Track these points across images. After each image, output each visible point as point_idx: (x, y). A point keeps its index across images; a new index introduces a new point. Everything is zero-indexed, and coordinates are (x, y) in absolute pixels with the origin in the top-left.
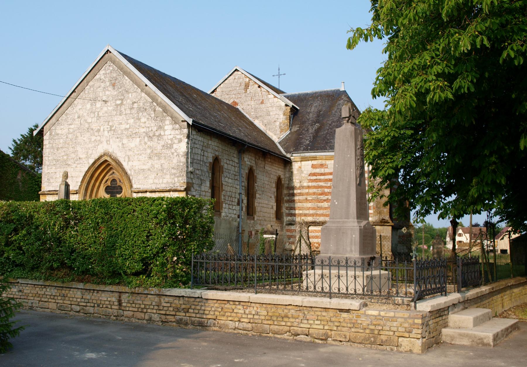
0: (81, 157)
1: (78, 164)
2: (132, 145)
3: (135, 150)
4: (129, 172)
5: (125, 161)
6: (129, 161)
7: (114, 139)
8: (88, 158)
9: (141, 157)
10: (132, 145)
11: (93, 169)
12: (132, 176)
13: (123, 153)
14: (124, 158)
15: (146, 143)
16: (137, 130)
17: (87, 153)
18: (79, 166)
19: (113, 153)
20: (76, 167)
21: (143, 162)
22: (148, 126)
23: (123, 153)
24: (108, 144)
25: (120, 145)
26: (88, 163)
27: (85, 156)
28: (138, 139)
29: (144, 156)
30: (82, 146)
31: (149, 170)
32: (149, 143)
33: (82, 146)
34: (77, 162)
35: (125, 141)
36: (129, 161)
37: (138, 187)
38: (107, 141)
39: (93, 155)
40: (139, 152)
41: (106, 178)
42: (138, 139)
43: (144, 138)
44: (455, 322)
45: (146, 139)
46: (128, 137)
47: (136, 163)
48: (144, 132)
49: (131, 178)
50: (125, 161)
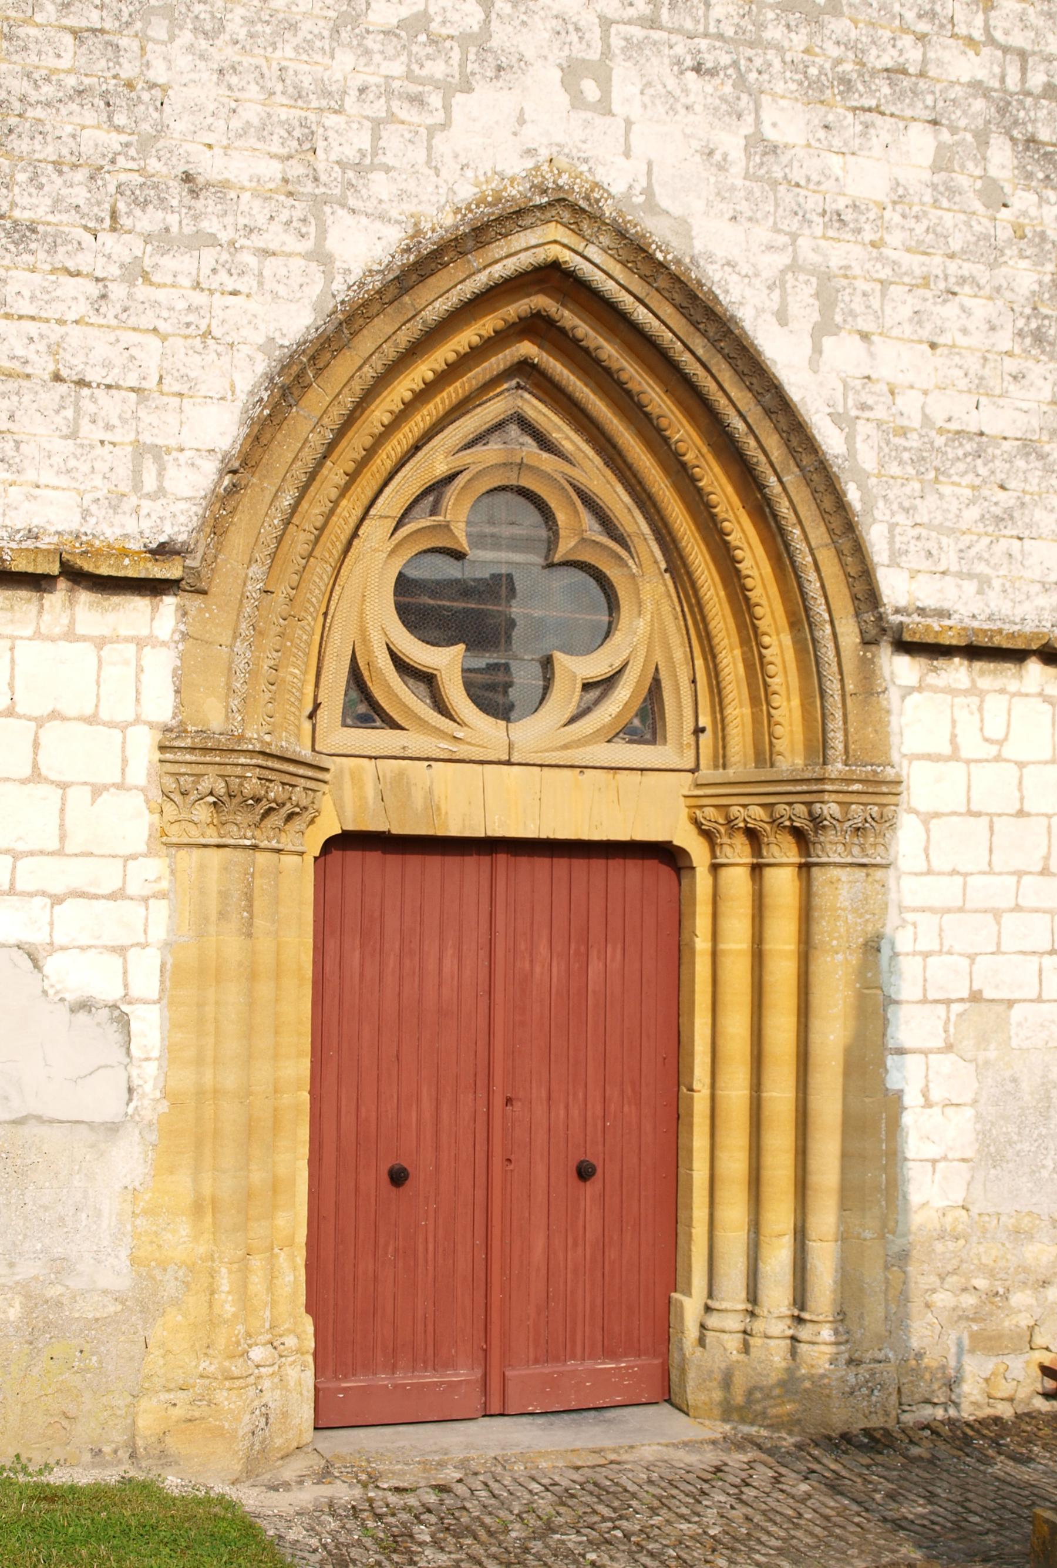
0: (210, 166)
1: (162, 240)
2: (865, 178)
3: (895, 239)
4: (831, 440)
5: (782, 318)
6: (825, 328)
7: (659, 68)
8: (310, 197)
9: (950, 310)
10: (865, 178)
11: (692, 351)
12: (862, 478)
13: (762, 234)
14: (777, 284)
15: (995, 198)
16: (913, 55)
17: (307, 142)
18: (177, 265)
19: (651, 206)
20: (138, 273)
21: (973, 363)
22: (1019, 40)
23: (762, 234)
24: (578, 101)
25: (731, 143)
26: (322, 257)
27: (272, 170)
28: (921, 143)
29: (981, 309)
30: (224, 52)
31: (1028, 447)
32: (1023, 201)
33: (224, 52)
34: (148, 220)
35: (786, 121)
36: (825, 328)
37: (929, 601)
38: (572, 72)
39: (380, 185)
40: (936, 263)
41: (436, 461)
42: (921, 143)
43: (982, 139)
44: (900, 1068)
45: (1001, 157)
46: (813, 90)
47: (896, 360)
48: (977, 87)
49: (853, 495)
50: (782, 318)
